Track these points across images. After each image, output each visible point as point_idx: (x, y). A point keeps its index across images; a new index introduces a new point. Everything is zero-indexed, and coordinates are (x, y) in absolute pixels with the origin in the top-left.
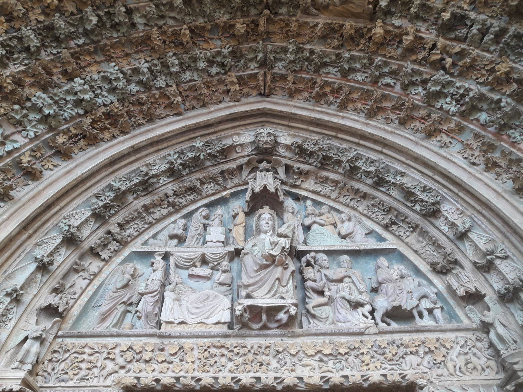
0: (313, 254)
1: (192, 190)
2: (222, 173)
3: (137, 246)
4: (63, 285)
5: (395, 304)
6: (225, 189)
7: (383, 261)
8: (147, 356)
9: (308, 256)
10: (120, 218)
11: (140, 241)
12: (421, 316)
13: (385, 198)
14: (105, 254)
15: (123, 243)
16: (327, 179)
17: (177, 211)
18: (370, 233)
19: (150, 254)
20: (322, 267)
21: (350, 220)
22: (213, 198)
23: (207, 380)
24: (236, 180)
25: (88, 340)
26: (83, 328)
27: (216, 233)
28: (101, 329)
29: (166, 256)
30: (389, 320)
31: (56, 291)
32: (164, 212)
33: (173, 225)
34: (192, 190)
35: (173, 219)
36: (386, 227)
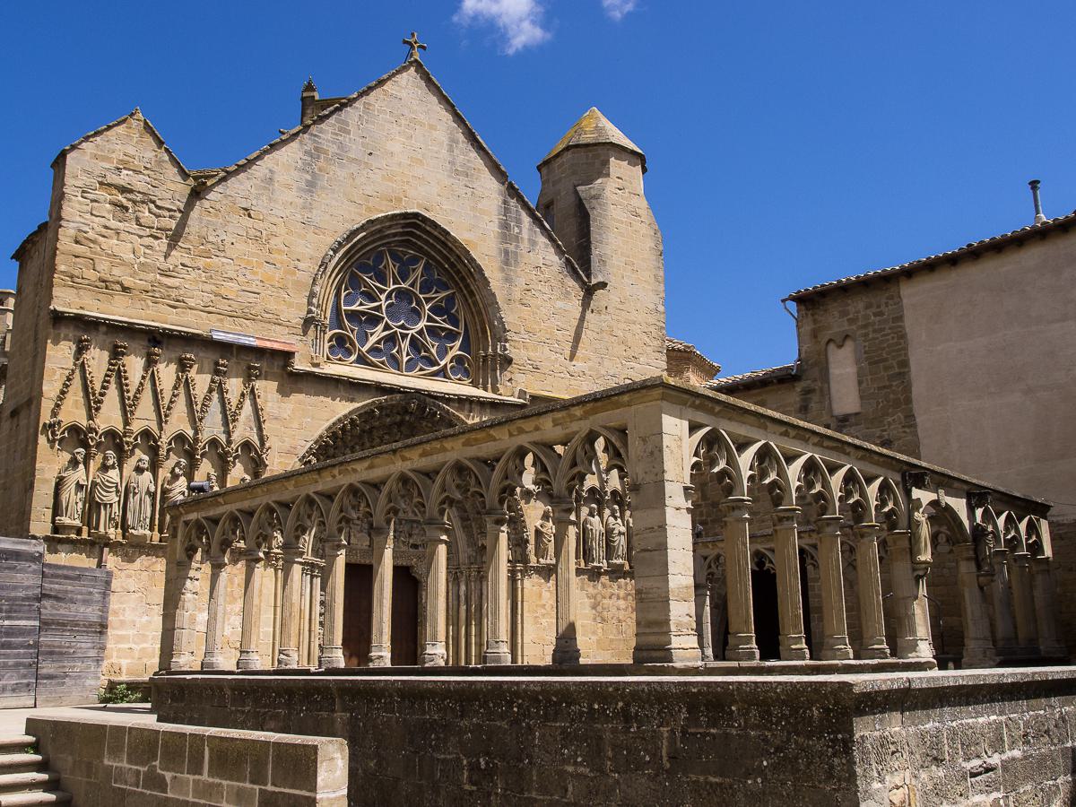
18: (414, 512)
23: (363, 562)
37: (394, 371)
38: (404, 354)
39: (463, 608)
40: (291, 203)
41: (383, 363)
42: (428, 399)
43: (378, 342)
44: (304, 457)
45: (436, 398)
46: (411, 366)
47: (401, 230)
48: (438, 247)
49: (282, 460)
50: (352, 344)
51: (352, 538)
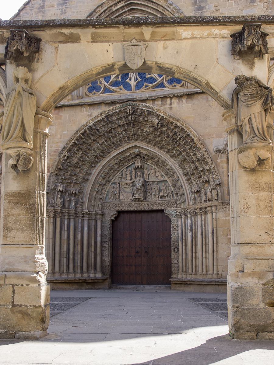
0: (149, 182)
1: (122, 165)
2: (128, 160)
3: (112, 181)
4: (101, 193)
5: (163, 195)
6: (129, 163)
7: (163, 184)
8: (119, 206)
9: (148, 183)
10: (108, 177)
11: (113, 180)
12: (168, 196)
13: (165, 168)
14: (107, 185)
15: (110, 181)
16: (153, 161)
17: (119, 171)
19: (116, 183)
20: (151, 185)
21: (159, 172)
22: (127, 166)
23: (129, 209)
24: (132, 161)
25: (109, 203)
26: (107, 201)
27: (129, 177)
28: (111, 200)
29: (119, 183)
30: (162, 197)
31: (100, 195)
32: (116, 172)
33: (119, 175)
34: (122, 165)
35: (119, 173)
36: (166, 175)
37: (128, 92)
38: (133, 80)
39: (190, 234)
40: (54, 14)
41: (121, 89)
42: (137, 103)
43: (117, 77)
44: (61, 153)
45: (144, 101)
46: (139, 86)
47: (124, 4)
48: (150, 5)
49: (52, 157)
50: (101, 83)
51: (121, 196)
